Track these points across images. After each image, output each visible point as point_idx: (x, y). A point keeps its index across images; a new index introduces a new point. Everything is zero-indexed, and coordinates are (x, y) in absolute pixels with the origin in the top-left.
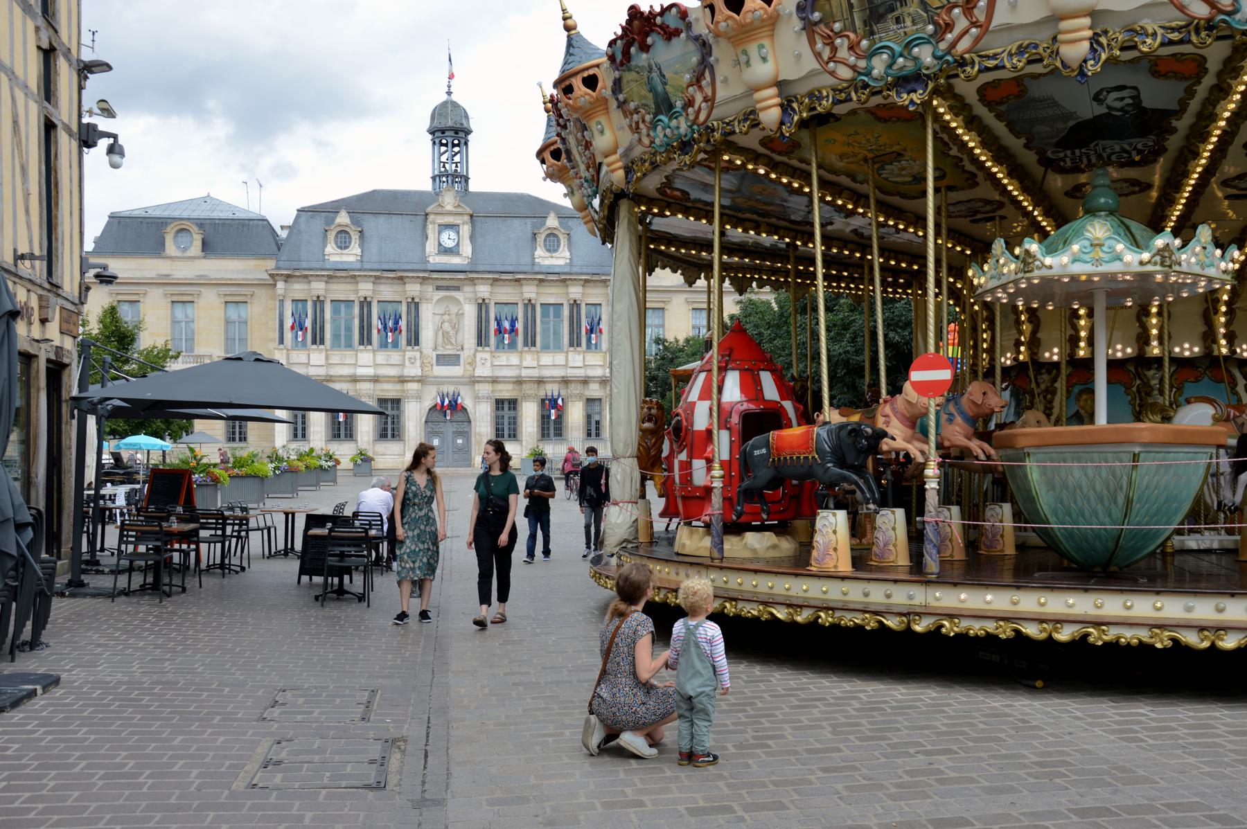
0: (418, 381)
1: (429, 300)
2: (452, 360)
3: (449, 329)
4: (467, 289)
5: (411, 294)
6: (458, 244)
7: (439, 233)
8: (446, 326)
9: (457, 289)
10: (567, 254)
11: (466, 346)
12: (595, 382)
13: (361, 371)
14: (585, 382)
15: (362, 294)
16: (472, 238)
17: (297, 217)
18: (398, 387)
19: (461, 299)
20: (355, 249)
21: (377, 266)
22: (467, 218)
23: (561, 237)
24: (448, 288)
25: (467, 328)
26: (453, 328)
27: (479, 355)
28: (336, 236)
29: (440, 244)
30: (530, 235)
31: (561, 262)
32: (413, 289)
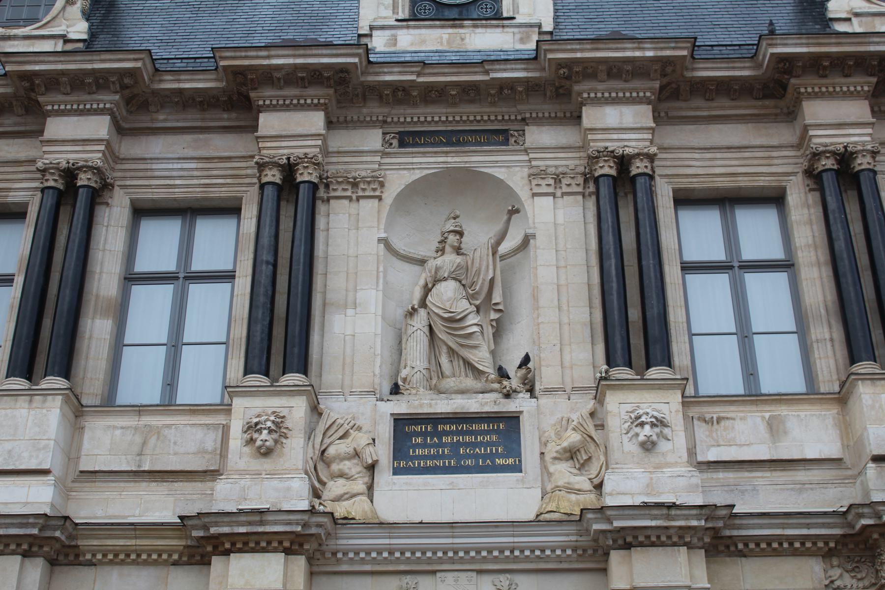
0: (291, 544)
3: (463, 306)
5: (283, 151)
8: (448, 294)
11: (547, 375)
24: (453, 139)
25: (548, 297)
26: (484, 303)
27: (619, 406)
32: (292, 129)
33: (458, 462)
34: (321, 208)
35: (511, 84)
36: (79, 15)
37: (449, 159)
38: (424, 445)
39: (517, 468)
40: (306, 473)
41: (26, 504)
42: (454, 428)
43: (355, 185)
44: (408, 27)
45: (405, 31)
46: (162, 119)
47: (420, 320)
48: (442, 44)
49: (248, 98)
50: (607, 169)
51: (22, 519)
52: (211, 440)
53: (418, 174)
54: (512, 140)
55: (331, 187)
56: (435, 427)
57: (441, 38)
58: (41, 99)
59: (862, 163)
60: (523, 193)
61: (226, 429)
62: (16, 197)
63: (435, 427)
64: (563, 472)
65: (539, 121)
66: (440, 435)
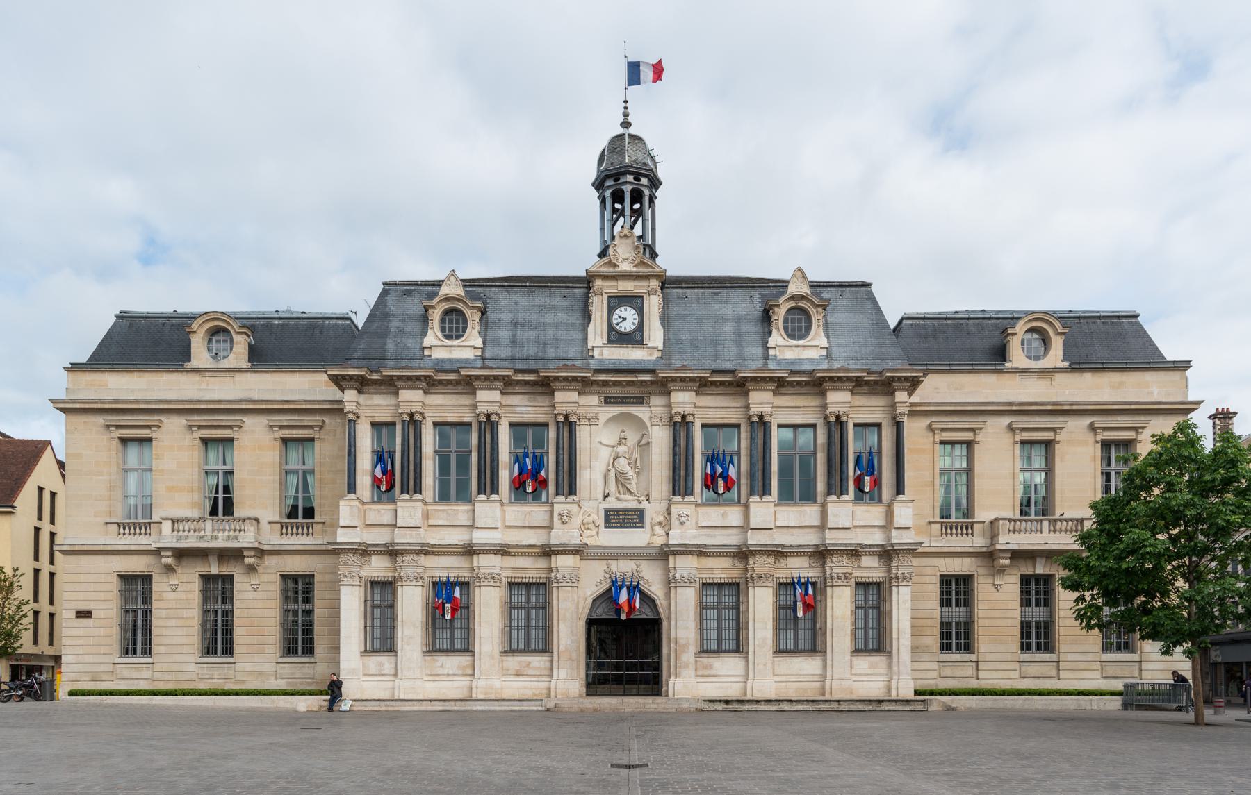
2: (633, 518)
4: (657, 401)
6: (640, 328)
7: (611, 310)
8: (623, 464)
9: (640, 401)
10: (823, 342)
12: (871, 554)
13: (479, 537)
14: (855, 553)
15: (482, 408)
16: (665, 319)
17: (384, 293)
18: (542, 563)
19: (646, 420)
20: (473, 338)
21: (507, 364)
22: (655, 284)
23: (813, 311)
24: (623, 401)
28: (443, 321)
30: (758, 314)
31: (814, 354)
32: (566, 399)
35: (645, 381)
46: (517, 389)
50: (678, 419)
51: (495, 545)
52: (547, 516)
59: (767, 419)
60: (648, 424)
61: (552, 513)
62: (467, 420)
64: (658, 529)
65: (655, 394)
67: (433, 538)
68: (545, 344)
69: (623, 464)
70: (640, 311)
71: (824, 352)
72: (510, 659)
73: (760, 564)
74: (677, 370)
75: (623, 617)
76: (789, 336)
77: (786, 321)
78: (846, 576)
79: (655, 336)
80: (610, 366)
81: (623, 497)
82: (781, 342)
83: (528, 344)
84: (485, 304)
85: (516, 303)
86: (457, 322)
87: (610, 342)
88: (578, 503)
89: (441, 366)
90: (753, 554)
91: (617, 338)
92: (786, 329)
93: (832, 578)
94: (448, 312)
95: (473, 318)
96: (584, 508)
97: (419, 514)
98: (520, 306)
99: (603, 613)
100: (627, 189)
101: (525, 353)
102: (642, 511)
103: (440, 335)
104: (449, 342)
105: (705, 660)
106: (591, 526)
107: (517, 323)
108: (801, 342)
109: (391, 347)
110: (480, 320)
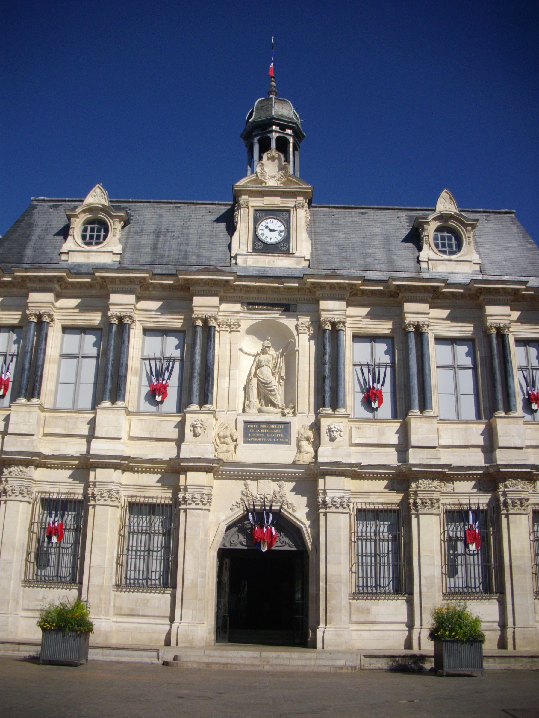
1: (233, 327)
2: (277, 432)
6: (287, 239)
7: (257, 221)
10: (476, 258)
16: (313, 233)
29: (256, 238)
31: (467, 268)
33: (267, 439)
34: (217, 334)
36: (118, 241)
37: (267, 316)
38: (254, 433)
39: (288, 443)
40: (213, 443)
41: (114, 450)
42: (265, 426)
43: (230, 326)
44: (252, 255)
45: (251, 256)
47: (254, 382)
48: (265, 263)
49: (189, 288)
53: (255, 321)
54: (291, 309)
55: (221, 326)
56: (259, 426)
57: (265, 261)
58: (109, 286)
63: (259, 426)
66: (260, 429)
67: (46, 447)
68: (186, 251)
69: (266, 373)
70: (287, 223)
71: (477, 268)
72: (125, 595)
73: (424, 488)
74: (327, 276)
75: (264, 549)
76: (440, 251)
77: (436, 238)
78: (522, 502)
79: (303, 246)
80: (255, 273)
81: (265, 408)
82: (432, 255)
83: (171, 249)
84: (129, 216)
85: (161, 216)
86: (99, 231)
87: (256, 251)
88: (213, 413)
89: (75, 270)
90: (417, 476)
91: (262, 247)
92: (437, 246)
93: (506, 504)
94: (88, 222)
95: (116, 226)
96: (221, 420)
97: (33, 420)
98: (164, 219)
99: (239, 542)
100: (275, 135)
101: (165, 260)
102: (288, 423)
103: (79, 240)
104: (87, 248)
105: (361, 603)
106: (228, 440)
107: (160, 232)
108: (453, 257)
109: (29, 252)
110: (123, 228)
